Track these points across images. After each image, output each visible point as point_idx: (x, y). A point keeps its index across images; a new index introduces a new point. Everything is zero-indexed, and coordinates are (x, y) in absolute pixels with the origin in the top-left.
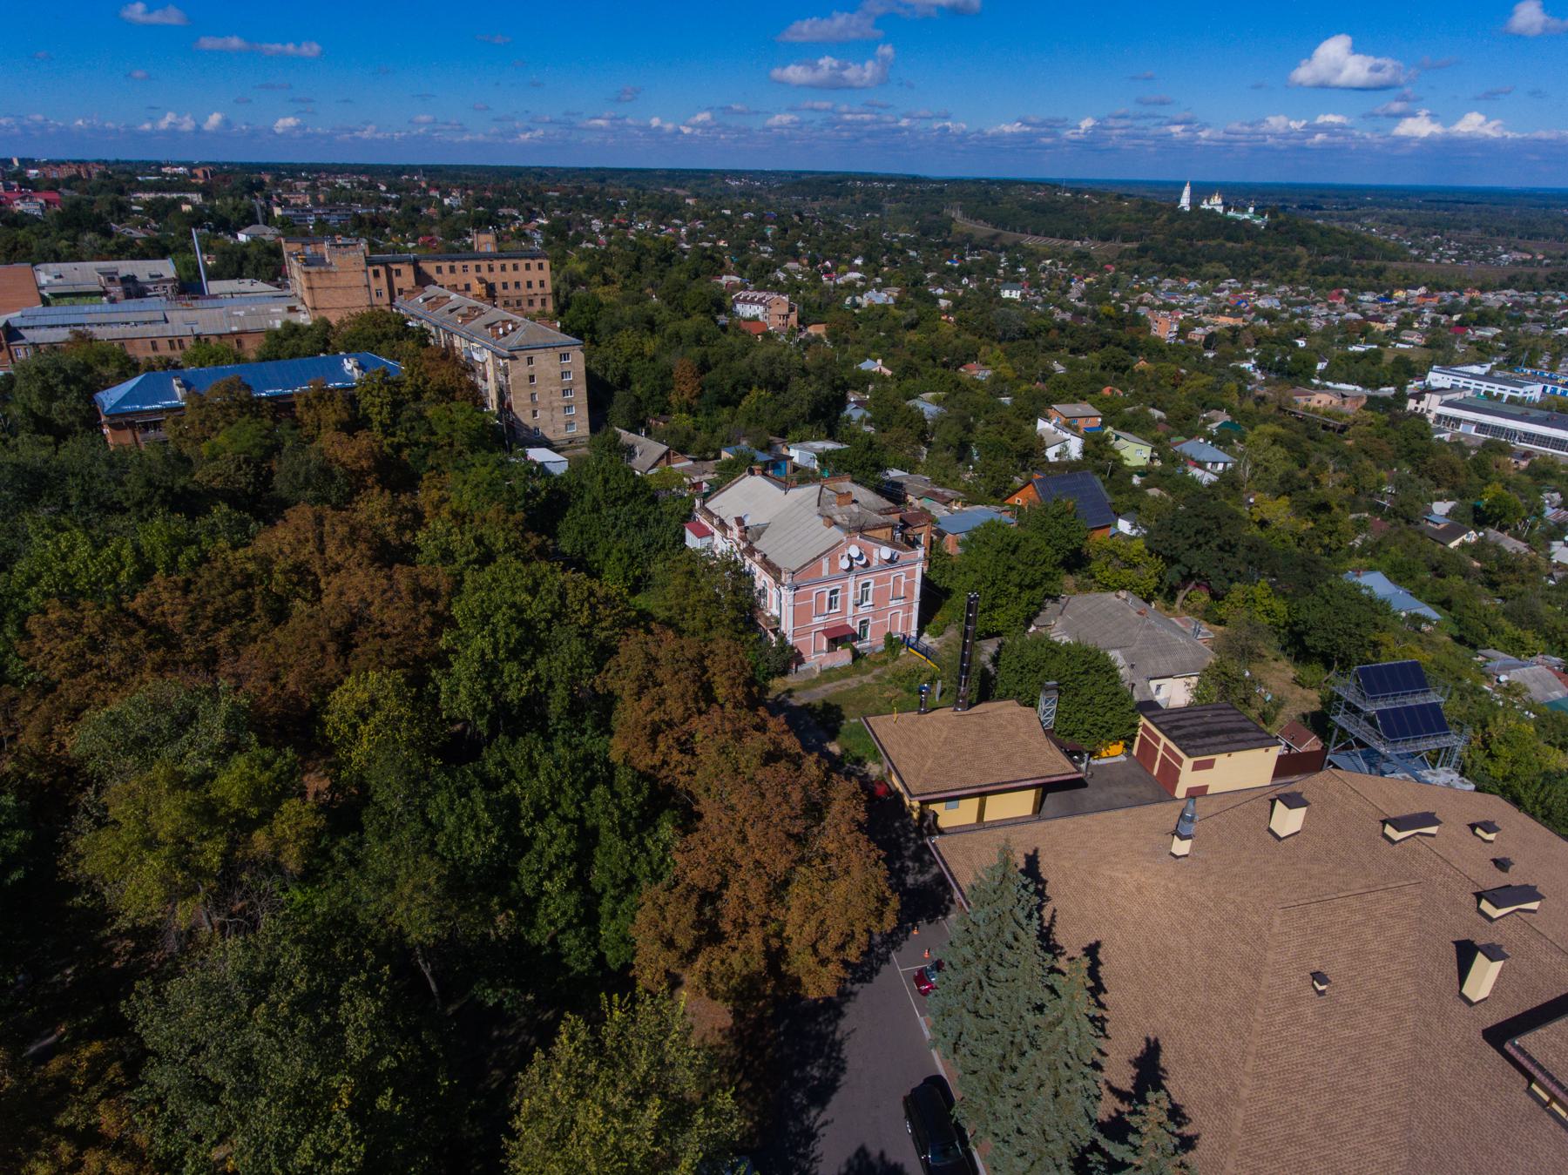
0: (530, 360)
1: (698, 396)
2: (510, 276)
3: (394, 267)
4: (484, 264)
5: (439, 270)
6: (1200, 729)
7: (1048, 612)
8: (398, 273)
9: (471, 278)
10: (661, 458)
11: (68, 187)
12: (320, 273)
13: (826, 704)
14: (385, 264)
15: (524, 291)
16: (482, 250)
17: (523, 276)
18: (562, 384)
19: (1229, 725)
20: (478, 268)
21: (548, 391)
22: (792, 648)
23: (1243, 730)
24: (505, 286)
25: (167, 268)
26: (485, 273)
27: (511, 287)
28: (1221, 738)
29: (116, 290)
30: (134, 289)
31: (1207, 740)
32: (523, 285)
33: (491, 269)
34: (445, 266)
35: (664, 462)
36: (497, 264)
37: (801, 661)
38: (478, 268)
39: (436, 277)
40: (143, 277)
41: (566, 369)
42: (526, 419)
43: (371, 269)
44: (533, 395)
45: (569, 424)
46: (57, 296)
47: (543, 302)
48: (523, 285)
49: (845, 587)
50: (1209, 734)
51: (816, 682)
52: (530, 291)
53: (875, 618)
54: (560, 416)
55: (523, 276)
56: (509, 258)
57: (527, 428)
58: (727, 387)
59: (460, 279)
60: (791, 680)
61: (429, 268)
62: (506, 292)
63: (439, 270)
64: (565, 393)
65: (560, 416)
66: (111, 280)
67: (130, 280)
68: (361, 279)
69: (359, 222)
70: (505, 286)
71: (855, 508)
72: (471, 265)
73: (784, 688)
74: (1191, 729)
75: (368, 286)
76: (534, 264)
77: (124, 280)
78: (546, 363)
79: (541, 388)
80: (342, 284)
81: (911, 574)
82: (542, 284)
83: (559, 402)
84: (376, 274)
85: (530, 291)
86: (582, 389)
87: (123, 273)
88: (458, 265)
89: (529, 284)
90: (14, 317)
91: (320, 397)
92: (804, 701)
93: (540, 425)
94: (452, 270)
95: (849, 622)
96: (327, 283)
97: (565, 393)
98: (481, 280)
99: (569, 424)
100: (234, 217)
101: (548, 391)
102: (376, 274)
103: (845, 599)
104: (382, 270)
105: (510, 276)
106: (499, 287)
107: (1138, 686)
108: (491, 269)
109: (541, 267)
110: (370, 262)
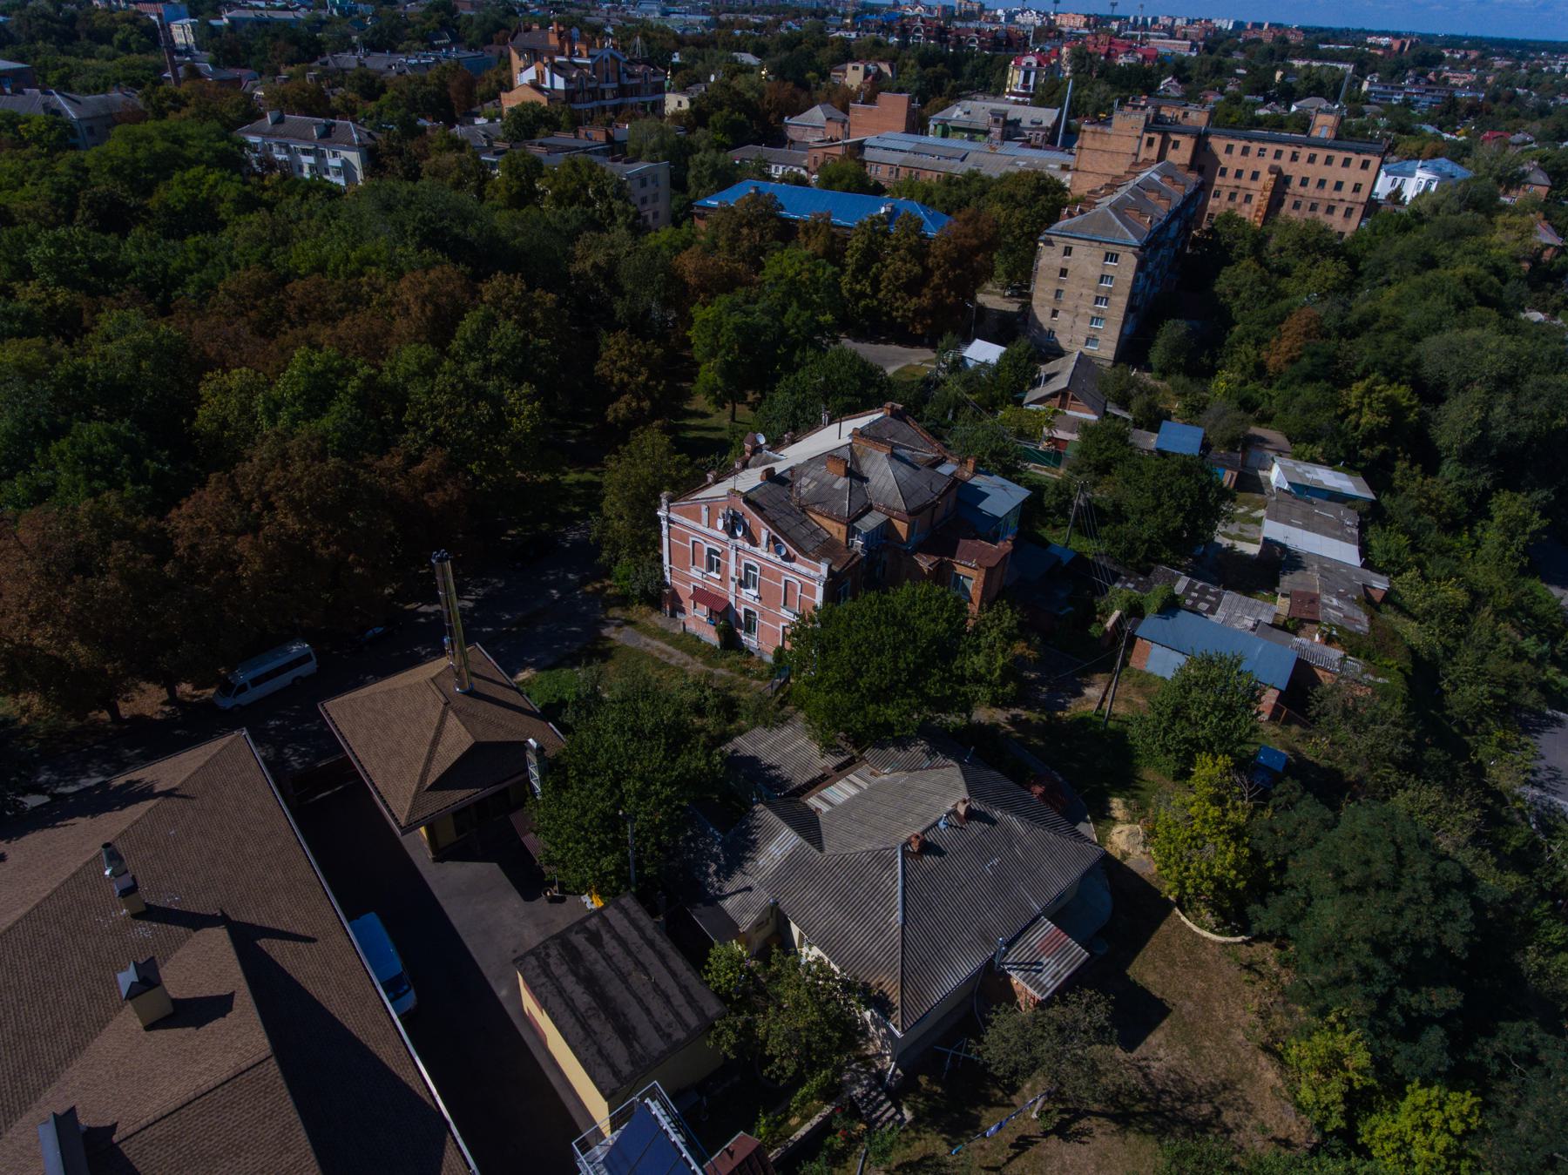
0: (1068, 251)
1: (1292, 361)
2: (1318, 170)
3: (1174, 137)
4: (1288, 151)
5: (1229, 149)
6: (600, 967)
7: (901, 755)
8: (1176, 145)
9: (1263, 165)
10: (1054, 395)
11: (1242, 51)
12: (1094, 133)
13: (611, 649)
14: (1165, 135)
15: (1328, 193)
16: (1314, 134)
17: (1334, 173)
18: (1097, 289)
19: (634, 1013)
20: (1278, 155)
21: (1079, 293)
22: (666, 585)
23: (626, 1033)
24: (1304, 182)
25: (1048, 116)
26: (1284, 164)
27: (1312, 185)
28: (582, 998)
29: (996, 130)
30: (1011, 130)
31: (570, 983)
32: (1330, 185)
33: (1294, 158)
34: (1239, 145)
36: (1305, 152)
37: (683, 611)
38: (1278, 155)
39: (1224, 159)
40: (1025, 123)
41: (1108, 272)
42: (1042, 314)
43: (1146, 136)
44: (1058, 293)
45: (1090, 340)
46: (956, 129)
47: (1348, 213)
48: (1330, 185)
49: (725, 554)
50: (590, 982)
51: (663, 634)
52: (1336, 195)
53: (762, 614)
54: (1083, 327)
55: (1334, 173)
56: (1340, 149)
57: (1040, 327)
58: (1359, 369)
59: (1250, 164)
60: (659, 620)
61: (1218, 144)
62: (1302, 190)
63: (1229, 149)
64: (1097, 300)
65: (1083, 327)
66: (996, 121)
67: (1016, 122)
68: (1132, 145)
69: (1450, 113)
70: (1304, 182)
71: (842, 483)
72: (1271, 148)
73: (634, 618)
74: (591, 954)
75: (1136, 155)
76: (1357, 160)
77: (1007, 123)
78: (1086, 260)
79: (1070, 287)
80: (1112, 147)
81: (812, 592)
82: (1357, 188)
83: (1087, 308)
84: (1150, 142)
85: (1336, 195)
86: (1120, 302)
87: (1010, 117)
88: (1255, 146)
89: (1322, 183)
90: (871, 140)
91: (815, 228)
92: (613, 636)
93: (1057, 329)
94: (1245, 151)
95: (732, 600)
96: (1097, 145)
97: (1097, 300)
98: (1272, 170)
99: (1090, 340)
100: (1301, 88)
101: (1079, 293)
102: (1150, 142)
103: (727, 566)
104: (1158, 138)
105: (1318, 170)
106: (1295, 183)
107: (752, 896)
108: (1294, 158)
109: (1365, 165)
110: (1147, 129)
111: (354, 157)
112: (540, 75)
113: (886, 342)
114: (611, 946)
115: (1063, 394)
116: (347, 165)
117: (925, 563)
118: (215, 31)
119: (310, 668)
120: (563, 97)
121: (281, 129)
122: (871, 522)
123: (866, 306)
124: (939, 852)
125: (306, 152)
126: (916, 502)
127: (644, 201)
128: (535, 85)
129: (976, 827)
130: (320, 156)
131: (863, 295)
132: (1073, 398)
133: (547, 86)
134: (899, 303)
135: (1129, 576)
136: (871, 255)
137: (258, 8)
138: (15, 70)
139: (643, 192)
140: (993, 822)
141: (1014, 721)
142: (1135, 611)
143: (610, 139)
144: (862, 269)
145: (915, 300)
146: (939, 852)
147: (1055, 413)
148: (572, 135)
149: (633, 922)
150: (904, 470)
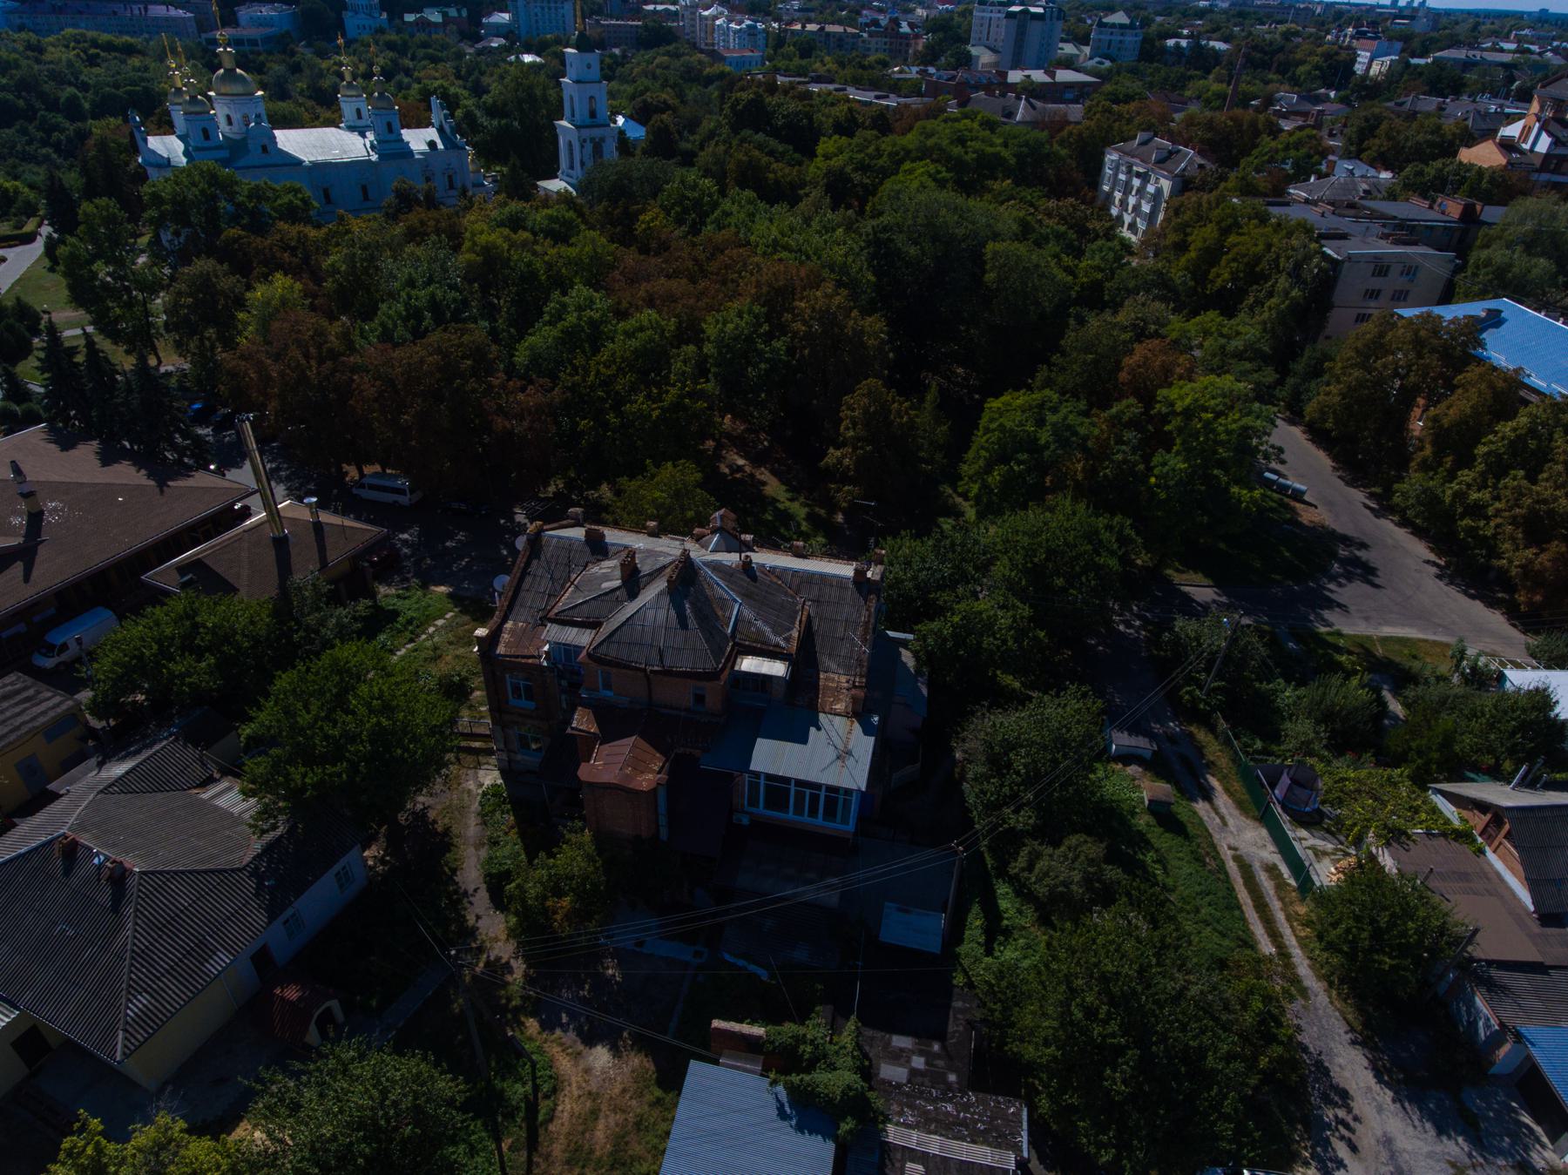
10: (1482, 807)
35: (1479, 820)
111: (1166, 185)
112: (1526, 131)
113: (1491, 603)
114: (17, 710)
115: (1497, 815)
116: (1159, 191)
117: (582, 721)
118: (1408, 65)
119: (404, 500)
120: (1538, 163)
121: (1144, 148)
122: (571, 635)
123: (1472, 531)
124: (67, 872)
125: (1138, 175)
126: (612, 652)
127: (1373, 294)
128: (1508, 146)
129: (105, 896)
130: (1145, 178)
131: (1477, 510)
132: (1508, 836)
133: (1526, 146)
134: (1507, 546)
135: (947, 1054)
136: (1530, 456)
137: (1502, 50)
138: (1084, 84)
139: (1376, 283)
140: (116, 907)
141: (498, 969)
142: (779, 1061)
143: (1469, 216)
144: (1498, 468)
145: (1529, 553)
146: (67, 872)
147: (1463, 836)
148: (1426, 204)
149: (44, 713)
150: (665, 615)
